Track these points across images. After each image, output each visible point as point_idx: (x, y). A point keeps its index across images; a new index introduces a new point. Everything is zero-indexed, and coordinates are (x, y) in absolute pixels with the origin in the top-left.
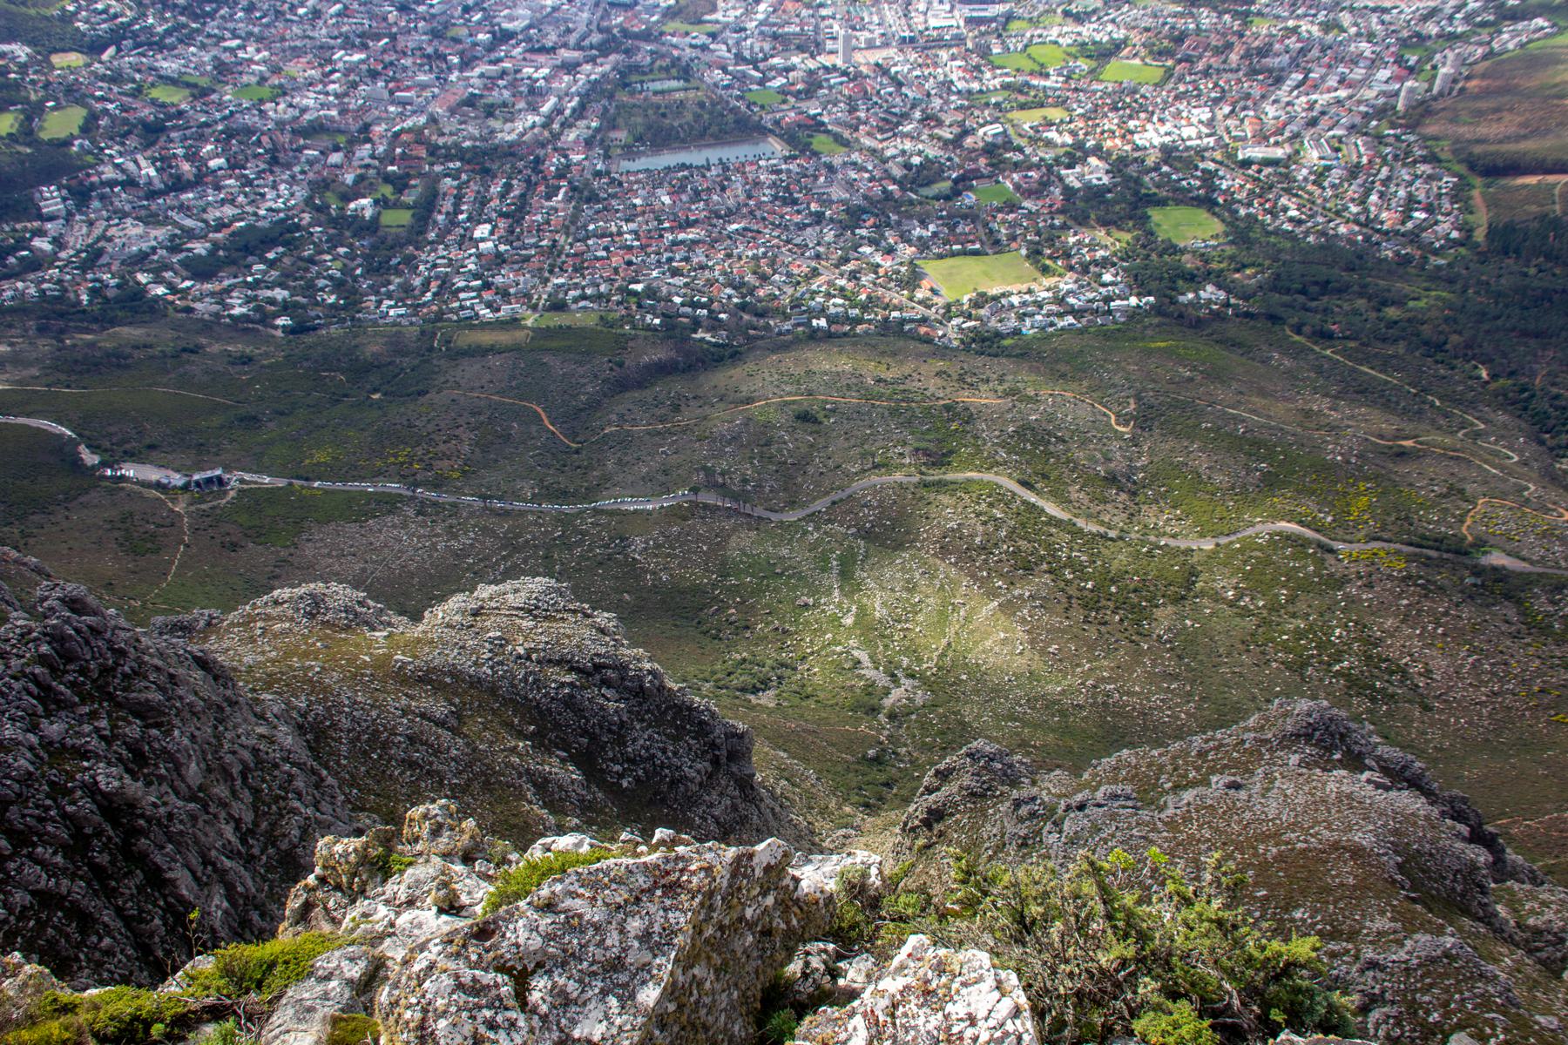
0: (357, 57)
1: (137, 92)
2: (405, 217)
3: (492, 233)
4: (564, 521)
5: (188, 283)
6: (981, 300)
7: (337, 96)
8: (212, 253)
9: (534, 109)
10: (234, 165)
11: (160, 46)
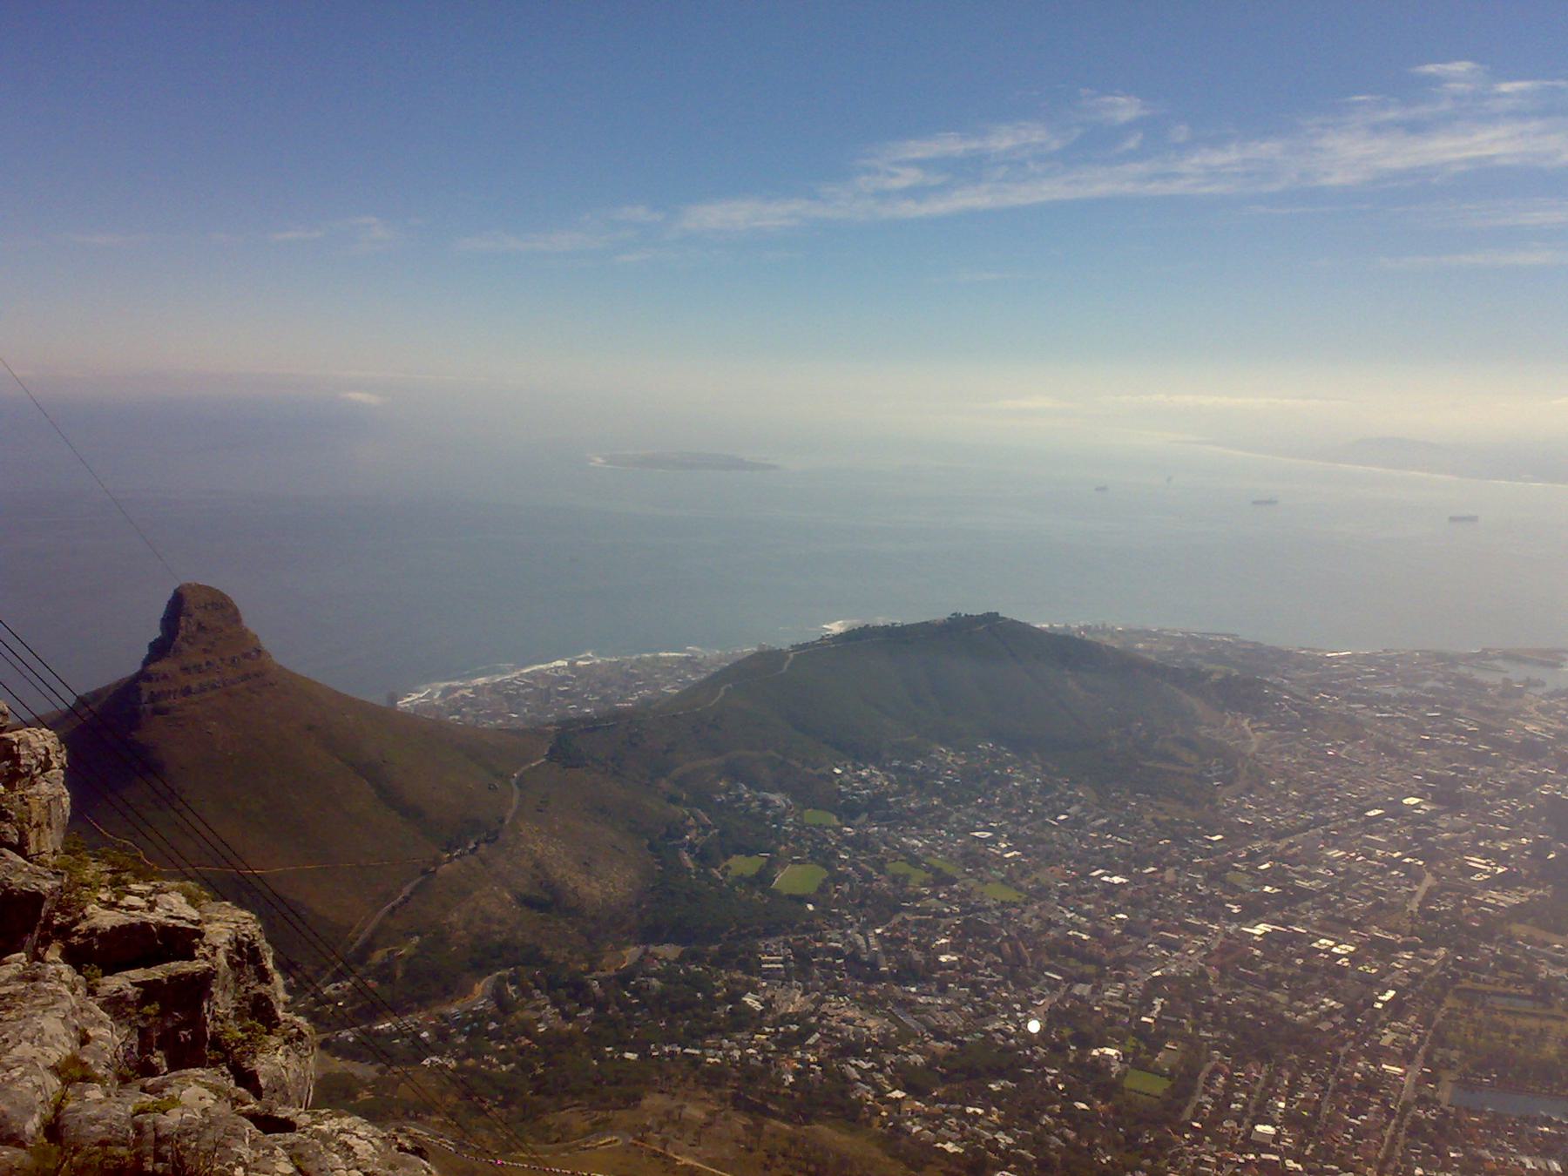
0: (1117, 880)
2: (1159, 1086)
3: (1277, 1138)
5: (898, 1094)
7: (1087, 914)
8: (929, 1066)
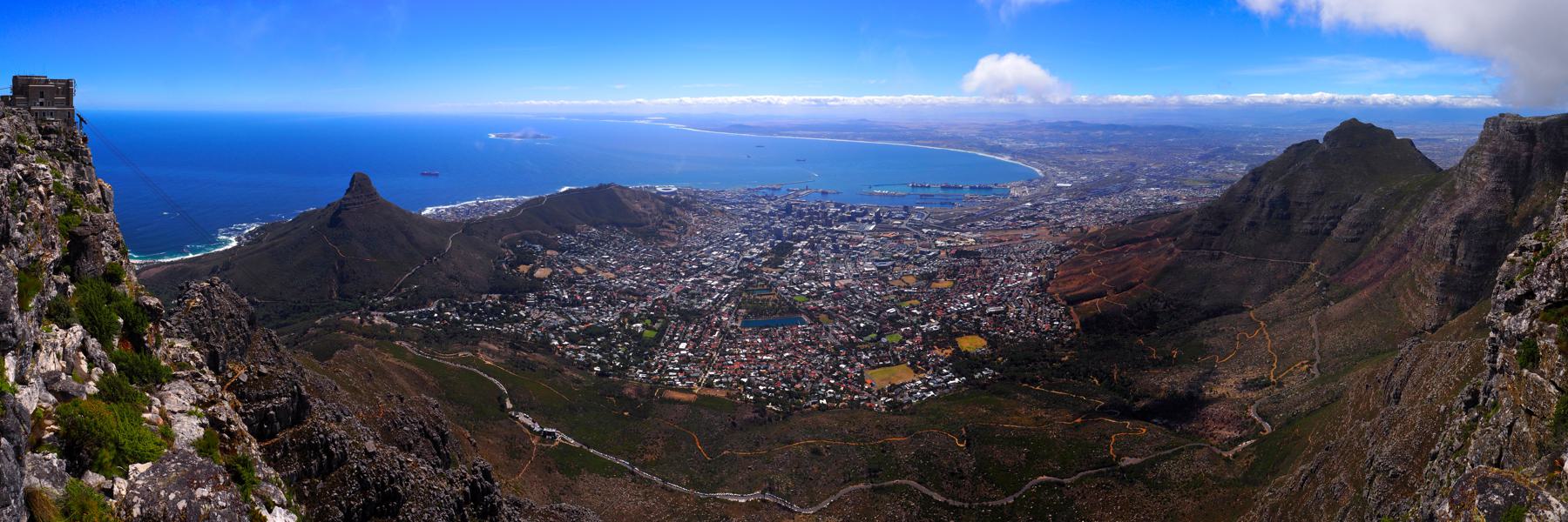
1: (570, 268)
4: (701, 502)
6: (893, 387)
9: (710, 296)
10: (595, 301)
11: (583, 254)
